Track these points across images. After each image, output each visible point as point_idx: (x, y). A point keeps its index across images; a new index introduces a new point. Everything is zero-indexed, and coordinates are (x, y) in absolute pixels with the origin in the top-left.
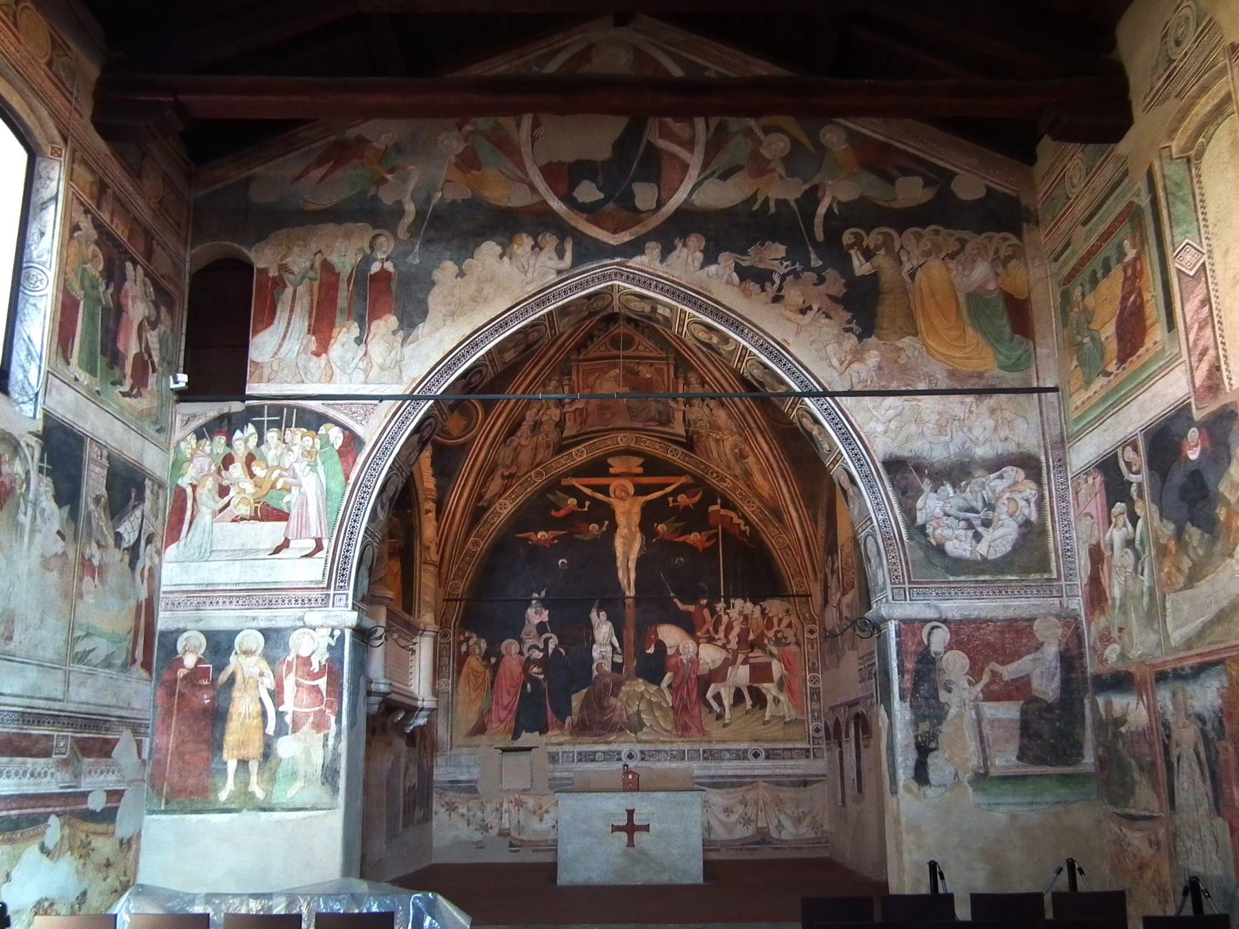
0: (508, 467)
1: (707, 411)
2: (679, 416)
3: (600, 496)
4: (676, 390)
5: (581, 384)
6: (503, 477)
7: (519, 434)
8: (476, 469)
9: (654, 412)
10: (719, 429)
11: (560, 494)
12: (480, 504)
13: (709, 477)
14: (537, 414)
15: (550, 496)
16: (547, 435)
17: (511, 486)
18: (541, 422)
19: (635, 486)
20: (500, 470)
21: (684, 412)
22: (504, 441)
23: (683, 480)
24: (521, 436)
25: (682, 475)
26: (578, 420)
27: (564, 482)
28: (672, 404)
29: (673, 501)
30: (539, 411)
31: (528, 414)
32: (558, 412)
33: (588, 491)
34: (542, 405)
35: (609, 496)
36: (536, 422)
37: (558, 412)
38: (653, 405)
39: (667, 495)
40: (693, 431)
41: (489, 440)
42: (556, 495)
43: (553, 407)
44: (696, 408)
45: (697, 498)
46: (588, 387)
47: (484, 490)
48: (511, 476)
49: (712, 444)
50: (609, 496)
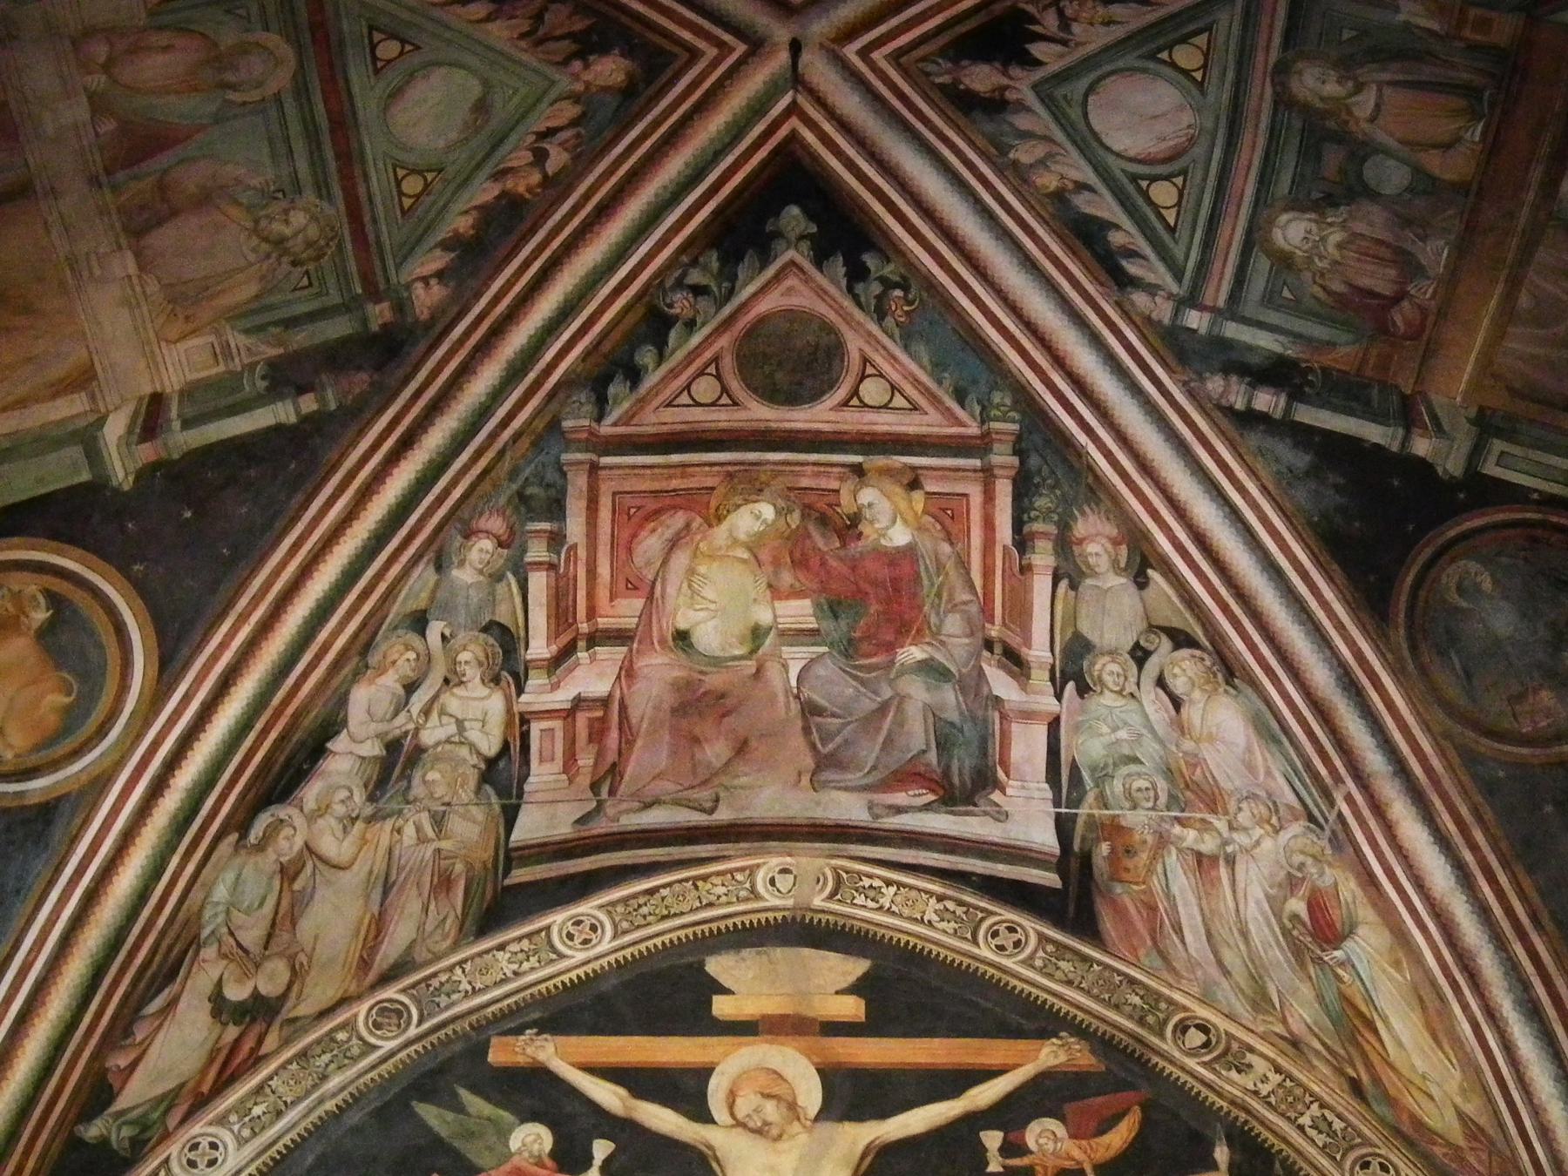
0: (247, 960)
1: (1154, 705)
2: (1028, 746)
3: (661, 1119)
4: (1019, 612)
5: (604, 570)
6: (219, 1006)
7: (311, 792)
8: (92, 939)
9: (917, 736)
10: (1213, 800)
11: (476, 1104)
12: (93, 1131)
13: (1168, 1046)
14: (402, 705)
15: (431, 1115)
16: (439, 821)
17: (256, 1060)
18: (419, 750)
19: (830, 1075)
20: (206, 972)
21: (1054, 725)
22: (240, 823)
23: (1049, 1055)
24: (322, 810)
25: (1043, 1034)
26: (586, 760)
27: (503, 1053)
28: (1001, 683)
29: (1008, 1149)
30: (411, 688)
31: (360, 697)
32: (495, 704)
33: (608, 1095)
34: (426, 662)
35: (704, 1116)
36: (393, 746)
37: (495, 704)
38: (917, 691)
39: (975, 1121)
40: (1091, 822)
41: (171, 802)
42: (459, 1108)
43: (473, 674)
44: (1108, 699)
45: (1118, 1138)
46: (632, 587)
47: (122, 1061)
48: (260, 1010)
49: (1181, 882)
50: (704, 1116)
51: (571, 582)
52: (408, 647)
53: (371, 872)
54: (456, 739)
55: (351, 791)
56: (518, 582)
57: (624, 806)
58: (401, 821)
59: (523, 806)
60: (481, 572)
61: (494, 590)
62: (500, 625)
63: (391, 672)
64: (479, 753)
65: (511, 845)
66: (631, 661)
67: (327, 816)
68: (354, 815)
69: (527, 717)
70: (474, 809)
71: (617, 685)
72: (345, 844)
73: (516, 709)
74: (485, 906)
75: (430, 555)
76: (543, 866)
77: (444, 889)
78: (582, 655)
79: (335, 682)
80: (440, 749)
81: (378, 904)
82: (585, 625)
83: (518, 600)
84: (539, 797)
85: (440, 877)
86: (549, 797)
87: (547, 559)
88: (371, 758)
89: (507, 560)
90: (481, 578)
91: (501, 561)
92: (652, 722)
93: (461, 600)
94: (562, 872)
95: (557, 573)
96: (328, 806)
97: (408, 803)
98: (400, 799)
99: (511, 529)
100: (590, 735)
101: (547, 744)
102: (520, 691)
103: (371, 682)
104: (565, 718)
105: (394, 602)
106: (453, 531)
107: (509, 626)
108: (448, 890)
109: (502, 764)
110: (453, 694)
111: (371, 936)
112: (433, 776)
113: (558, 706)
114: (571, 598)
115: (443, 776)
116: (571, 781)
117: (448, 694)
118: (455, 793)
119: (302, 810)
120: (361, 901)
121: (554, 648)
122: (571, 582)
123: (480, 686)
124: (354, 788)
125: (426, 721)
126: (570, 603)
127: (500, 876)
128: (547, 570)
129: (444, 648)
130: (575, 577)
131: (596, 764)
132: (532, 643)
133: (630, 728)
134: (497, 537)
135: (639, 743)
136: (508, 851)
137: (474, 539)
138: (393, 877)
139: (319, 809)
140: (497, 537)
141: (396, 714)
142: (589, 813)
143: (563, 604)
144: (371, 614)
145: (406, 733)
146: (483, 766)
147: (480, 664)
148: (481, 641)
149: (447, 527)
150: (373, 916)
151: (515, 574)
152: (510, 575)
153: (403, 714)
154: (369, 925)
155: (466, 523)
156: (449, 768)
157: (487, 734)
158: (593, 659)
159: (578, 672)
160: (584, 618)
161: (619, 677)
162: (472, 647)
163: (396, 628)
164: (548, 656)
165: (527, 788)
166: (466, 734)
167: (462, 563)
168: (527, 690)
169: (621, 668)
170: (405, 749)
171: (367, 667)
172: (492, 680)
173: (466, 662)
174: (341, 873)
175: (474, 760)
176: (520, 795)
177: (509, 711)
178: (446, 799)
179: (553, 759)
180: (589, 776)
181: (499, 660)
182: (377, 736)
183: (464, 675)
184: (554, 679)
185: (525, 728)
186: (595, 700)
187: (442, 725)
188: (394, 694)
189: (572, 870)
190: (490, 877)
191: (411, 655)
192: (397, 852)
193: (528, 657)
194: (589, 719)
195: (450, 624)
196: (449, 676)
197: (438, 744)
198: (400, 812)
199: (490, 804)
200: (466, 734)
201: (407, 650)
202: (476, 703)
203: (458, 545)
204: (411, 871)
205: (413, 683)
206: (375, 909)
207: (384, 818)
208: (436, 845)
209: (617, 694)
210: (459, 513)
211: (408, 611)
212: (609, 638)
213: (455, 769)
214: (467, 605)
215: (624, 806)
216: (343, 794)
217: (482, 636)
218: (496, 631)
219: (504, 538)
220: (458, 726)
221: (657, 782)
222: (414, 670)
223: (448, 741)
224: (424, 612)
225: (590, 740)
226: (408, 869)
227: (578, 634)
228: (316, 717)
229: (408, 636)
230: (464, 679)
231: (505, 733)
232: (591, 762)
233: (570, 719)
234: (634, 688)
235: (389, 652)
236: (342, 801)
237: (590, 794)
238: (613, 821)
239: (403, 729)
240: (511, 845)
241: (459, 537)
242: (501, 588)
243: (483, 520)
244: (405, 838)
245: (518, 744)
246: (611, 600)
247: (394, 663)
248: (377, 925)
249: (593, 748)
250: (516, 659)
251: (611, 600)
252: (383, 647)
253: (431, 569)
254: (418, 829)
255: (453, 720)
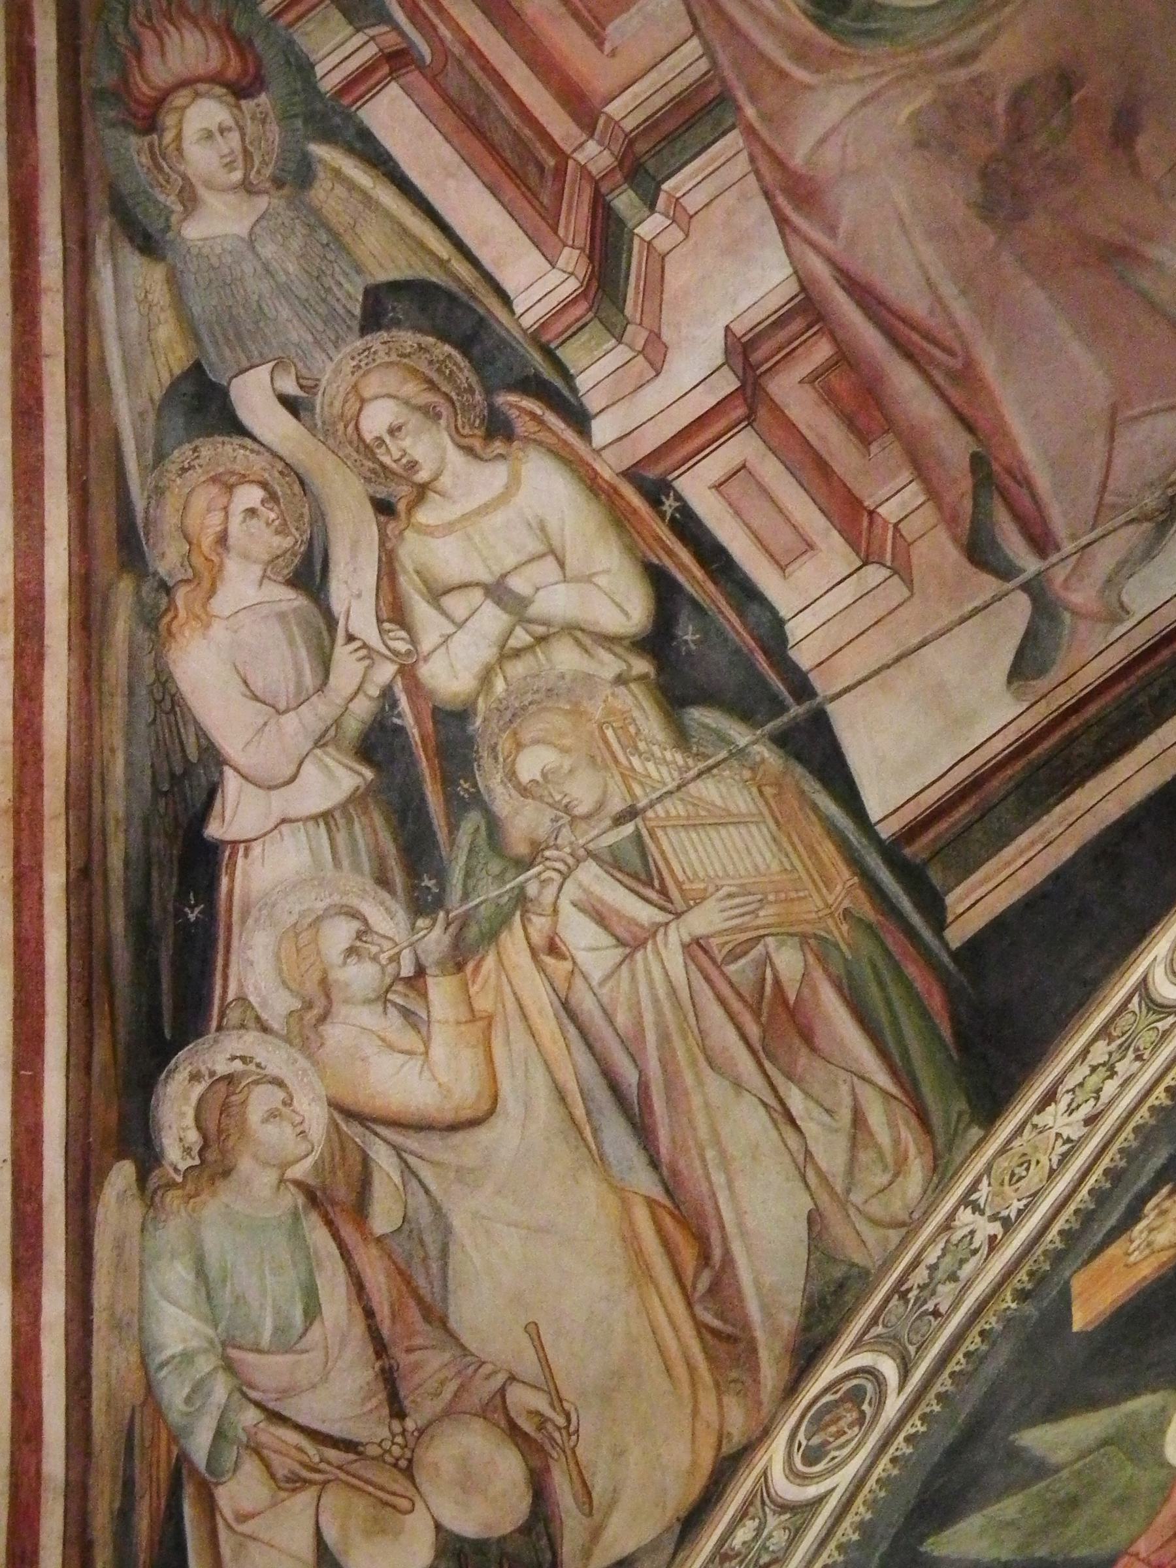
51: (472, 65)
52: (227, 484)
53: (562, 1097)
54: (521, 637)
55: (355, 914)
56: (351, 150)
57: (1105, 559)
58: (539, 925)
59: (830, 708)
60: (247, 188)
61: (315, 212)
62: (396, 287)
63: (232, 566)
64: (608, 640)
65: (886, 831)
66: (779, 163)
67: (341, 1011)
68: (407, 970)
69: (652, 473)
70: (708, 790)
71: (794, 241)
72: (438, 1051)
73: (607, 474)
74: (946, 1031)
75: (103, 229)
76: (1023, 840)
77: (797, 1041)
78: (649, 227)
79: (116, 666)
80: (500, 686)
81: (639, 1160)
82: (592, 147)
83: (387, 197)
84: (851, 666)
85: (757, 1014)
86: (879, 649)
87: (371, 50)
88: (344, 806)
89: (285, 118)
90: (262, 202)
91: (274, 131)
92: (967, 283)
93: (257, 287)
94: (1090, 828)
95: (421, 67)
96: (324, 983)
97: (522, 864)
98: (495, 867)
99: (226, 32)
100: (850, 422)
101: (762, 517)
102: (580, 420)
103: (205, 621)
104: (750, 419)
105: (108, 393)
106: (109, 134)
107: (425, 275)
108: (807, 1037)
109: (688, 633)
110: (427, 531)
111: (688, 1255)
112: (530, 766)
113: (705, 401)
114: (505, 108)
115: (564, 750)
116: (902, 570)
117: (408, 534)
118: (630, 774)
119: (265, 1029)
120: (590, 1184)
121: (570, 257)
122: (472, 65)
123: (475, 467)
124: (354, 902)
125: (413, 641)
126: (515, 120)
127: (927, 934)
128: (393, 74)
129: (312, 429)
130: (470, 46)
131: (933, 494)
132: (510, 282)
133: (928, 336)
134: (215, 79)
135: (988, 362)
136: (890, 852)
137: (170, 120)
138: (629, 1076)
139: (309, 1005)
140: (215, 79)
141: (325, 664)
142: (1030, 638)
143: (500, 136)
144: (78, 456)
145: (387, 693)
146: (642, 666)
147: (430, 413)
148: (382, 358)
149: (88, 131)
150: (651, 1203)
151: (329, 136)
152: (319, 150)
153: (343, 655)
154: (660, 1230)
155: (121, 93)
156: (560, 722)
157: (588, 579)
158: (681, 218)
159: (677, 277)
160: (574, 129)
161: (782, 221)
162: (372, 386)
163: (160, 457)
164: (572, 285)
165: (804, 657)
166: (533, 611)
167: (190, 199)
168: (593, 403)
169: (768, 195)
170: (414, 733)
171: (165, 588)
172: (489, 436)
173: (393, 431)
174: (483, 1135)
175: (609, 665)
176: (802, 688)
177: (592, 484)
178: (617, 805)
179: (810, 546)
180: (942, 536)
181: (466, 375)
182: (320, 742)
183: (413, 466)
184: (637, 335)
185: (669, 505)
186: (780, 321)
187: (460, 626)
188: (282, 616)
189: (1112, 811)
190: (894, 940)
191: (251, 496)
192: (586, 1004)
193: (528, 321)
194: (812, 379)
195: (280, 364)
196: (381, 493)
197: (486, 678)
198: (521, 899)
199: (740, 754)
200: (533, 611)
201: (230, 488)
202: (498, 518)
203: (145, 159)
204: (664, 1039)
205: (308, 558)
206: (645, 1182)
207: (492, 936)
208: (675, 936)
209: (819, 268)
210: (88, 84)
211: (157, 396)
212: (670, 138)
213: (577, 712)
214: (284, 291)
215: (1105, 559)
216: (340, 933)
217: (376, 340)
218: (398, 308)
219: (233, 70)
220: (499, 602)
221: (1125, 437)
222: (282, 531)
223: (507, 654)
224: (197, 368)
225: (864, 439)
226: (651, 1037)
227: (596, 184)
228: (129, 782)
229: (206, 452)
230: (423, 476)
231: (630, 549)
232: (913, 494)
233: (762, 412)
234: (844, 225)
235: (192, 523)
236: (351, 951)
237: (990, 584)
238: (1115, 620)
239: (375, 692)
240: (886, 831)
241: (134, 140)
242: (323, 193)
243: (152, 61)
244: (582, 957)
245: (685, 556)
246: (599, 41)
247: (222, 539)
248: (682, 1221)
249: (887, 451)
250: (503, 344)
251: (599, 41)
252: (169, 518)
253: (133, 261)
254: (600, 916)
255: (477, 595)
